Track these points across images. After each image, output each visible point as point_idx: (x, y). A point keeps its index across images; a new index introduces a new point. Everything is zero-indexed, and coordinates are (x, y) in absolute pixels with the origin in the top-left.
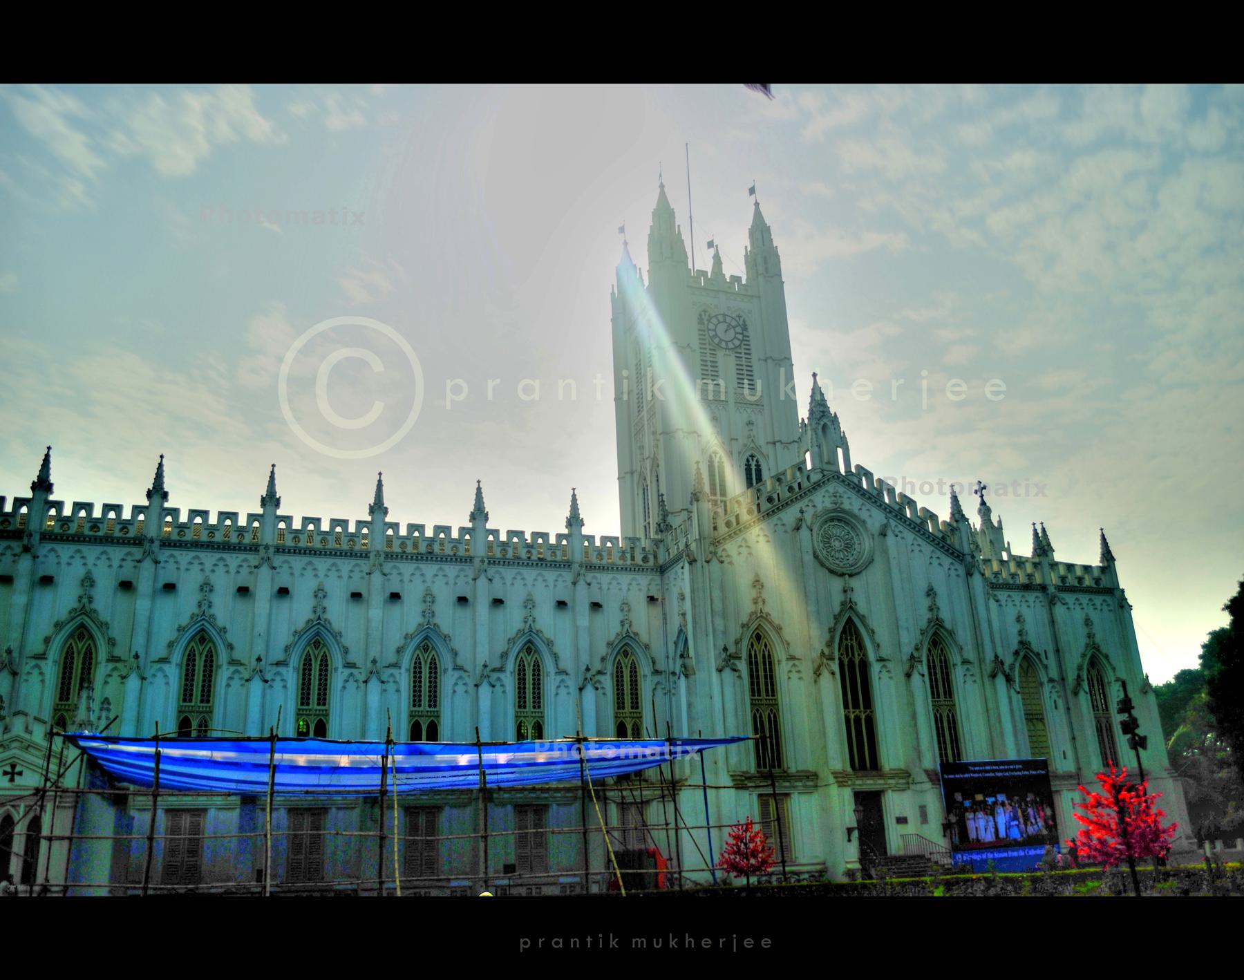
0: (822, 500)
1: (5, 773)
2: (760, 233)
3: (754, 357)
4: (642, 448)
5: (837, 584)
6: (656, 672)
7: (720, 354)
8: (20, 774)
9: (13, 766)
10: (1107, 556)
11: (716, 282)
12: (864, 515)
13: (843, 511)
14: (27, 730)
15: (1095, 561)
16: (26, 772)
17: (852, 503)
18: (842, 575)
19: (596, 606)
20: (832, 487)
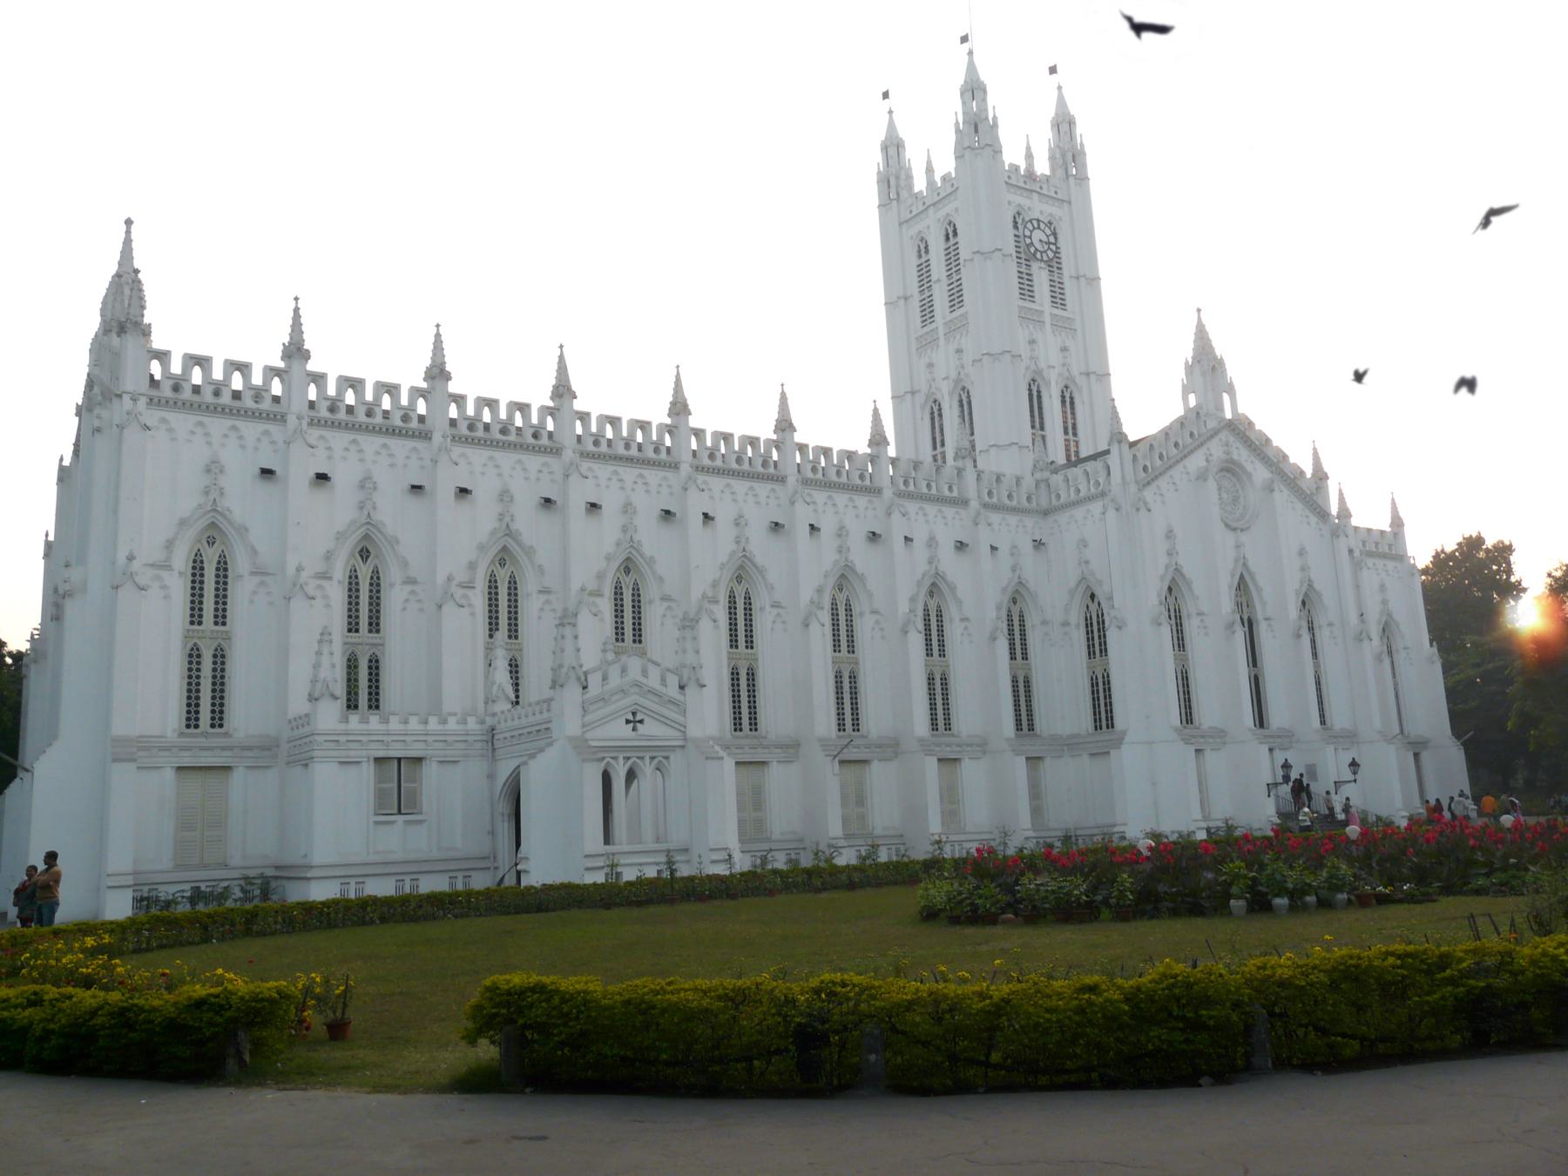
0: (1216, 449)
1: (628, 722)
2: (1064, 124)
3: (1066, 272)
4: (930, 365)
5: (1230, 538)
6: (1045, 623)
7: (1035, 266)
8: (641, 722)
9: (634, 714)
10: (1397, 522)
11: (1027, 182)
12: (1249, 467)
13: (1232, 461)
14: (645, 673)
15: (1385, 526)
16: (647, 720)
17: (1242, 455)
18: (1234, 530)
19: (993, 548)
20: (1223, 435)
